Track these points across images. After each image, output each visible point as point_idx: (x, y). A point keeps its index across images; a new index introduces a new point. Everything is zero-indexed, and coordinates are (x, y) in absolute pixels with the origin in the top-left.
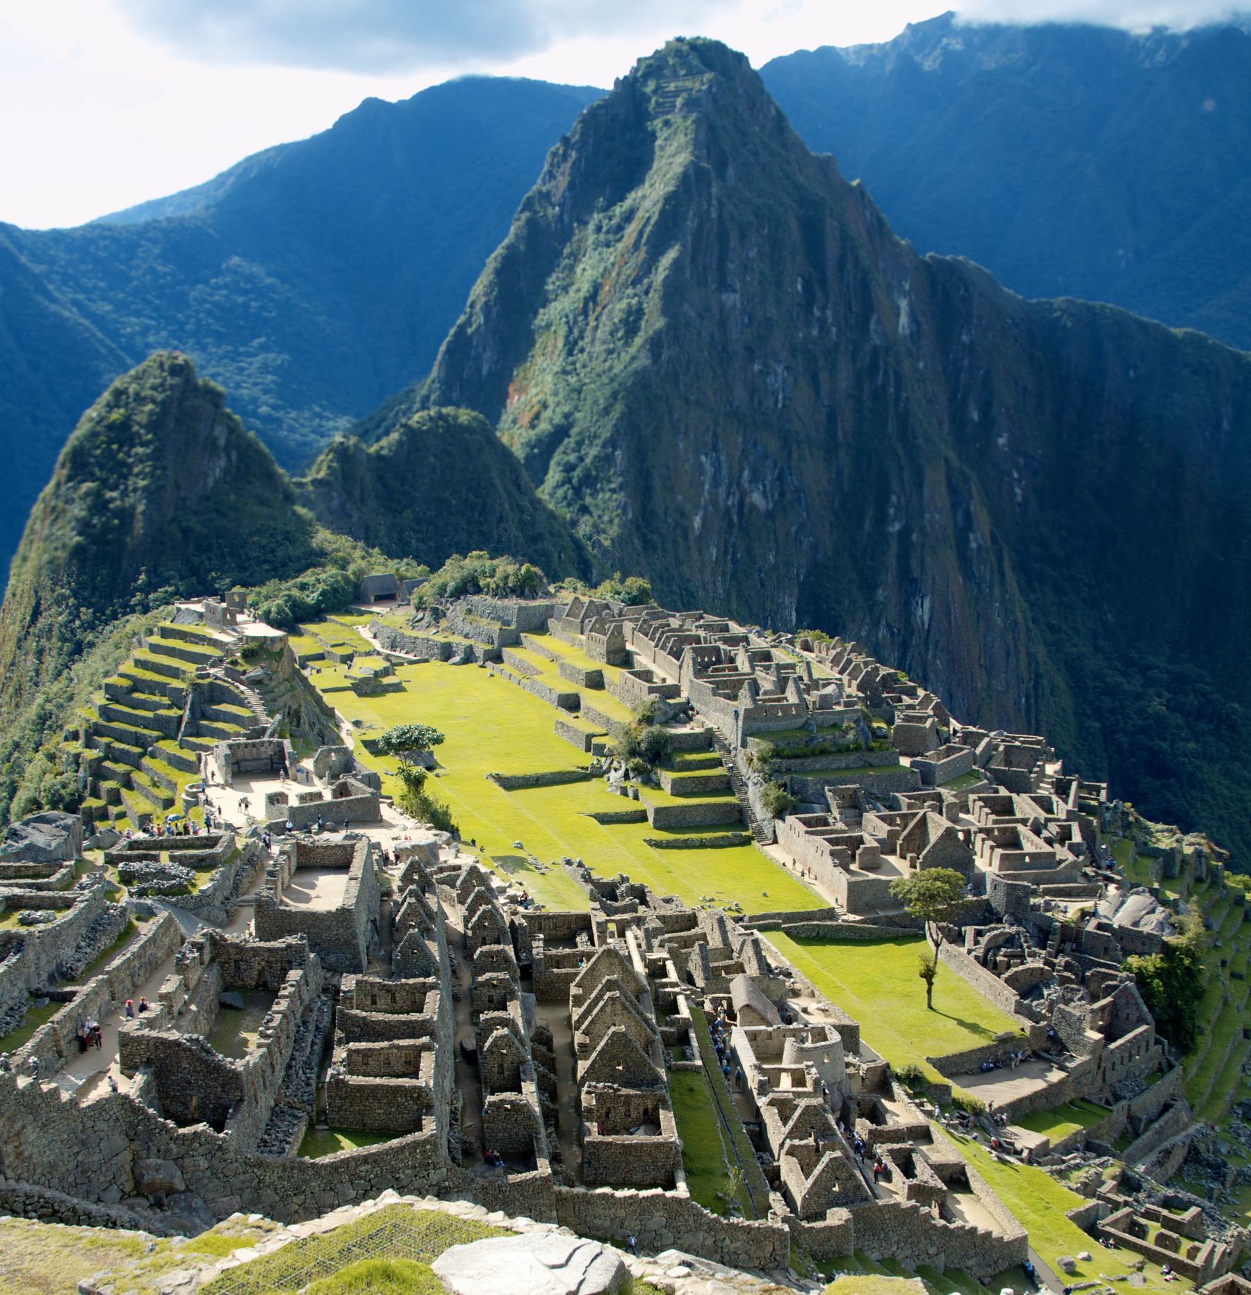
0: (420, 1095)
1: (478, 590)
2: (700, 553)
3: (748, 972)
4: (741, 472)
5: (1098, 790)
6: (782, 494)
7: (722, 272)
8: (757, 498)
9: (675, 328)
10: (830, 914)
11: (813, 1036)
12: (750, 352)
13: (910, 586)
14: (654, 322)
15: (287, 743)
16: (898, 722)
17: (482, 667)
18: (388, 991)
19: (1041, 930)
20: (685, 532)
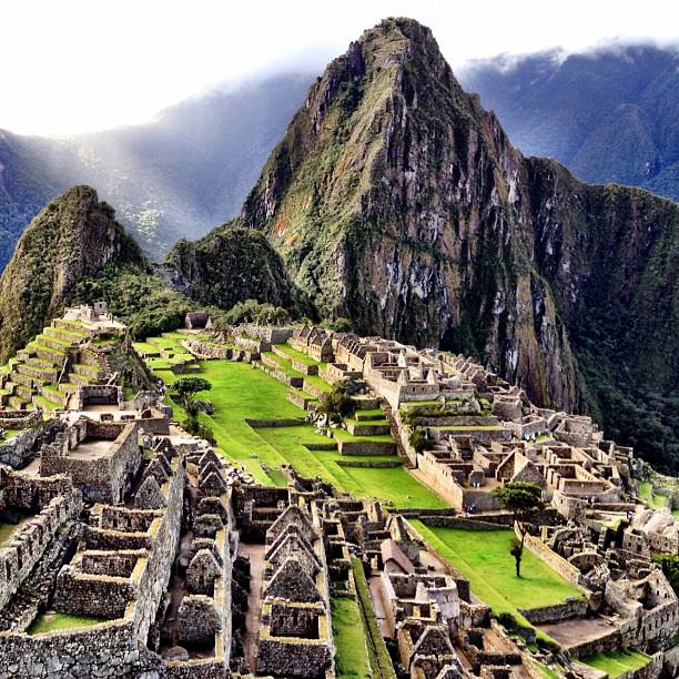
0: (127, 590)
1: (250, 321)
2: (384, 319)
3: (394, 538)
4: (411, 273)
5: (627, 452)
6: (433, 289)
7: (406, 159)
8: (418, 291)
9: (376, 193)
10: (452, 512)
11: (437, 583)
12: (419, 207)
13: (505, 344)
14: (366, 184)
15: (119, 388)
16: (496, 401)
17: (250, 363)
18: (126, 518)
19: (593, 530)
20: (375, 306)
